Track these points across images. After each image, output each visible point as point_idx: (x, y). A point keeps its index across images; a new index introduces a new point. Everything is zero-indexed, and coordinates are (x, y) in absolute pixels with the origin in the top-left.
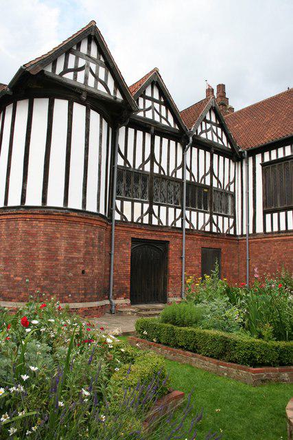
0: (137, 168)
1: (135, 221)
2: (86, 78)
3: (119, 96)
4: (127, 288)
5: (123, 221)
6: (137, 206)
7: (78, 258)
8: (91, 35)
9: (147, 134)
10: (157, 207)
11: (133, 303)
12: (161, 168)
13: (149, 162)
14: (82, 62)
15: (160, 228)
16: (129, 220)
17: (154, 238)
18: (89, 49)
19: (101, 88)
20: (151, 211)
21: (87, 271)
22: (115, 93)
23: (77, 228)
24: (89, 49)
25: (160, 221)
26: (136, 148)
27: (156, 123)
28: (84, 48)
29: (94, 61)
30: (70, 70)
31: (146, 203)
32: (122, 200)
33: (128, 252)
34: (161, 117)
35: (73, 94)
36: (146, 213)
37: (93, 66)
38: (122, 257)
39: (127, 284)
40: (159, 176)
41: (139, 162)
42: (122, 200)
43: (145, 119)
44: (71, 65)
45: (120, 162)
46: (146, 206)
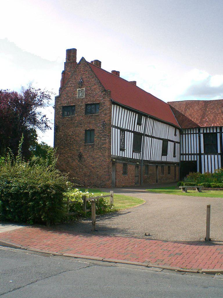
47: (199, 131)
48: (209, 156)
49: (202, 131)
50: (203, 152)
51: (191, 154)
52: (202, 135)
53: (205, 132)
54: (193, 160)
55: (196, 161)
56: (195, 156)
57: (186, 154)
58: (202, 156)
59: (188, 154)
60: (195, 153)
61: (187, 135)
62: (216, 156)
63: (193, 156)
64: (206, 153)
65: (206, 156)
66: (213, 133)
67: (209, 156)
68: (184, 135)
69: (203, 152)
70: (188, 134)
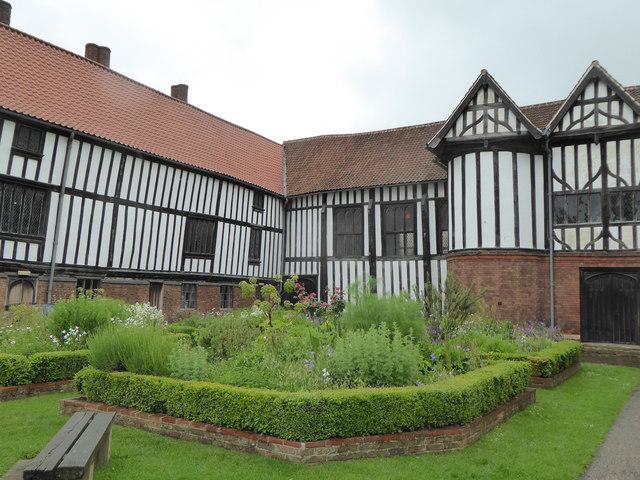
0: (581, 187)
1: (582, 248)
2: (486, 127)
3: (523, 129)
4: (575, 322)
5: (566, 252)
6: (585, 232)
7: (493, 292)
8: (485, 83)
9: (593, 145)
10: (616, 228)
11: (582, 340)
12: (619, 180)
13: (600, 177)
14: (480, 114)
15: (622, 253)
16: (574, 248)
17: (613, 265)
18: (486, 97)
19: (502, 130)
20: (606, 235)
21: (504, 303)
22: (518, 126)
23: (492, 265)
24: (486, 97)
25: (621, 245)
26: (576, 167)
27: (602, 128)
28: (480, 99)
29: (492, 106)
30: (469, 127)
31: (598, 225)
32: (563, 228)
33: (575, 284)
34: (609, 116)
35: (476, 146)
36: (599, 238)
37: (491, 112)
38: (567, 291)
39: (576, 318)
40: (617, 192)
41: (583, 180)
42: (563, 228)
43: (582, 130)
44: (470, 121)
45: (557, 187)
46: (598, 230)
47: (325, 201)
48: (345, 264)
49: (329, 202)
50: (330, 252)
51: (307, 259)
52: (330, 211)
53: (337, 203)
54: (309, 273)
55: (317, 276)
56: (315, 263)
57: (295, 259)
58: (330, 264)
59: (301, 259)
60: (315, 255)
61: (299, 212)
62: (360, 263)
63: (309, 263)
64: (339, 255)
65: (337, 263)
66: (355, 206)
67: (345, 264)
68: (294, 213)
69: (330, 252)
70: (302, 209)
